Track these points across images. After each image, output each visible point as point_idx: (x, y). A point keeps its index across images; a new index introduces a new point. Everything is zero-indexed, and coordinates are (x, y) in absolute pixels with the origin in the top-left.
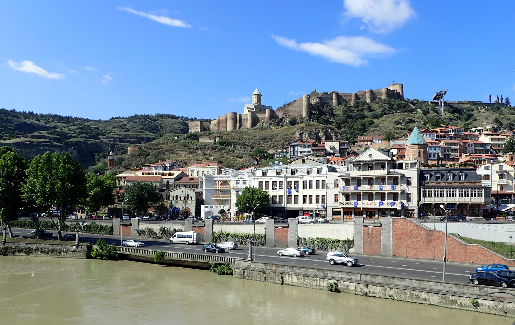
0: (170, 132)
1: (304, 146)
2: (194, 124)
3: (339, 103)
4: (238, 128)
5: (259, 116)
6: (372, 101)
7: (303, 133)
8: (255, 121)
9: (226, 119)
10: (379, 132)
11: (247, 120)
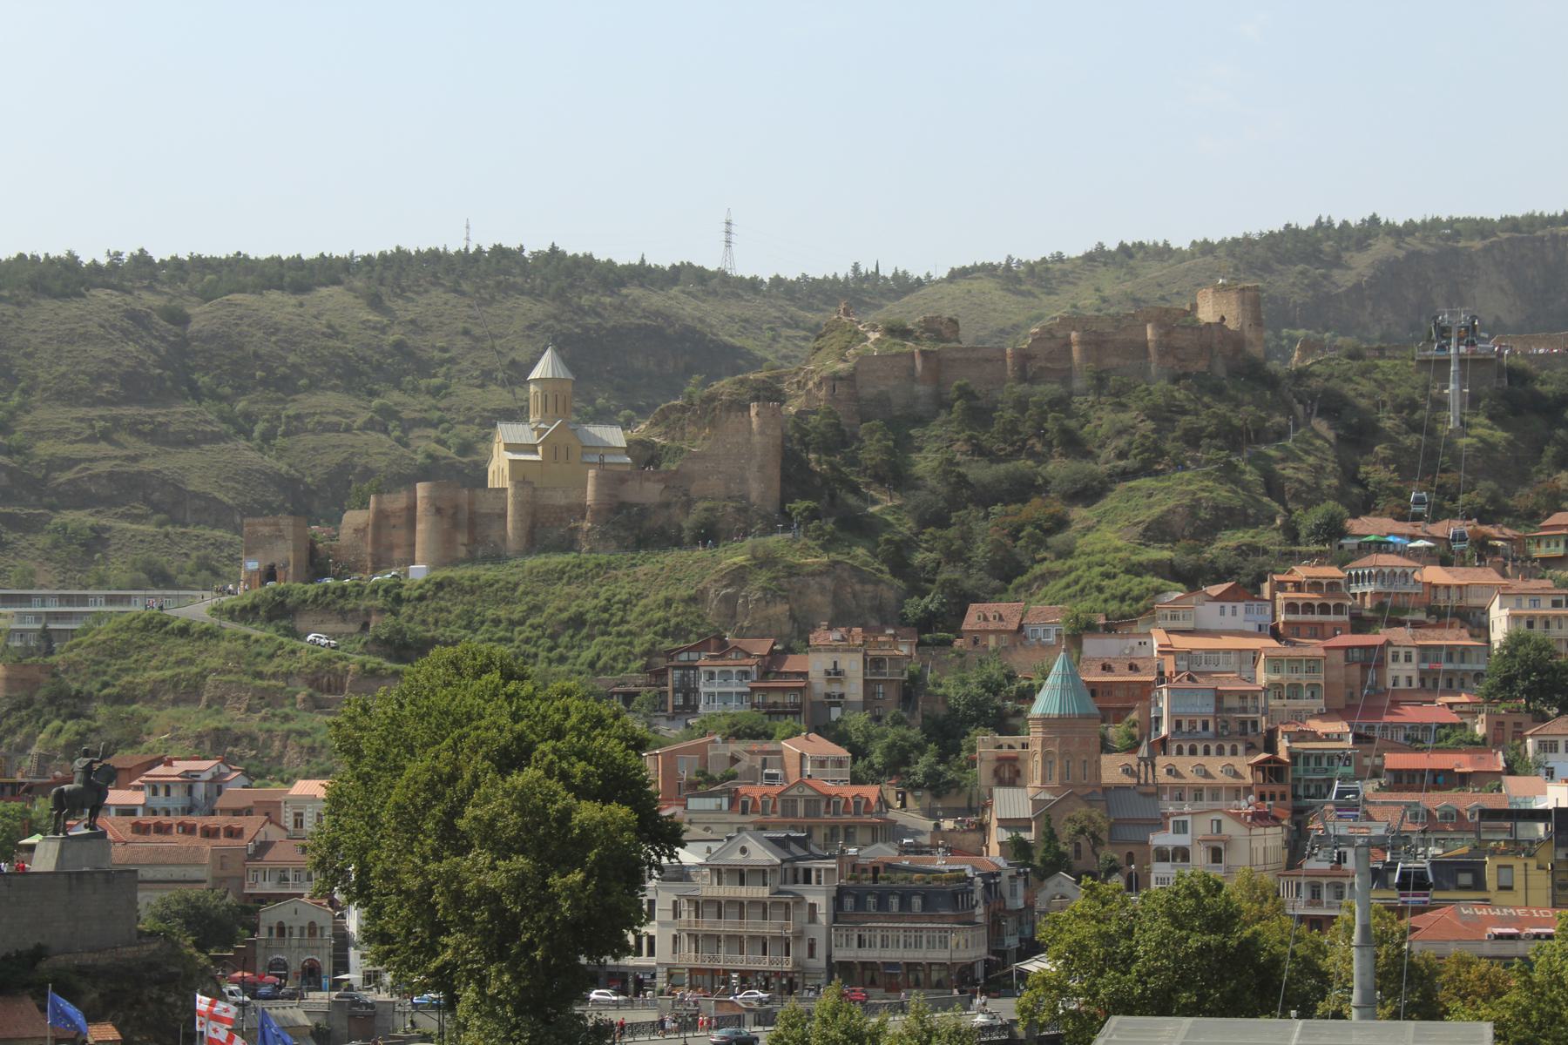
2: (266, 530)
4: (462, 552)
7: (734, 597)
9: (412, 508)
11: (503, 516)
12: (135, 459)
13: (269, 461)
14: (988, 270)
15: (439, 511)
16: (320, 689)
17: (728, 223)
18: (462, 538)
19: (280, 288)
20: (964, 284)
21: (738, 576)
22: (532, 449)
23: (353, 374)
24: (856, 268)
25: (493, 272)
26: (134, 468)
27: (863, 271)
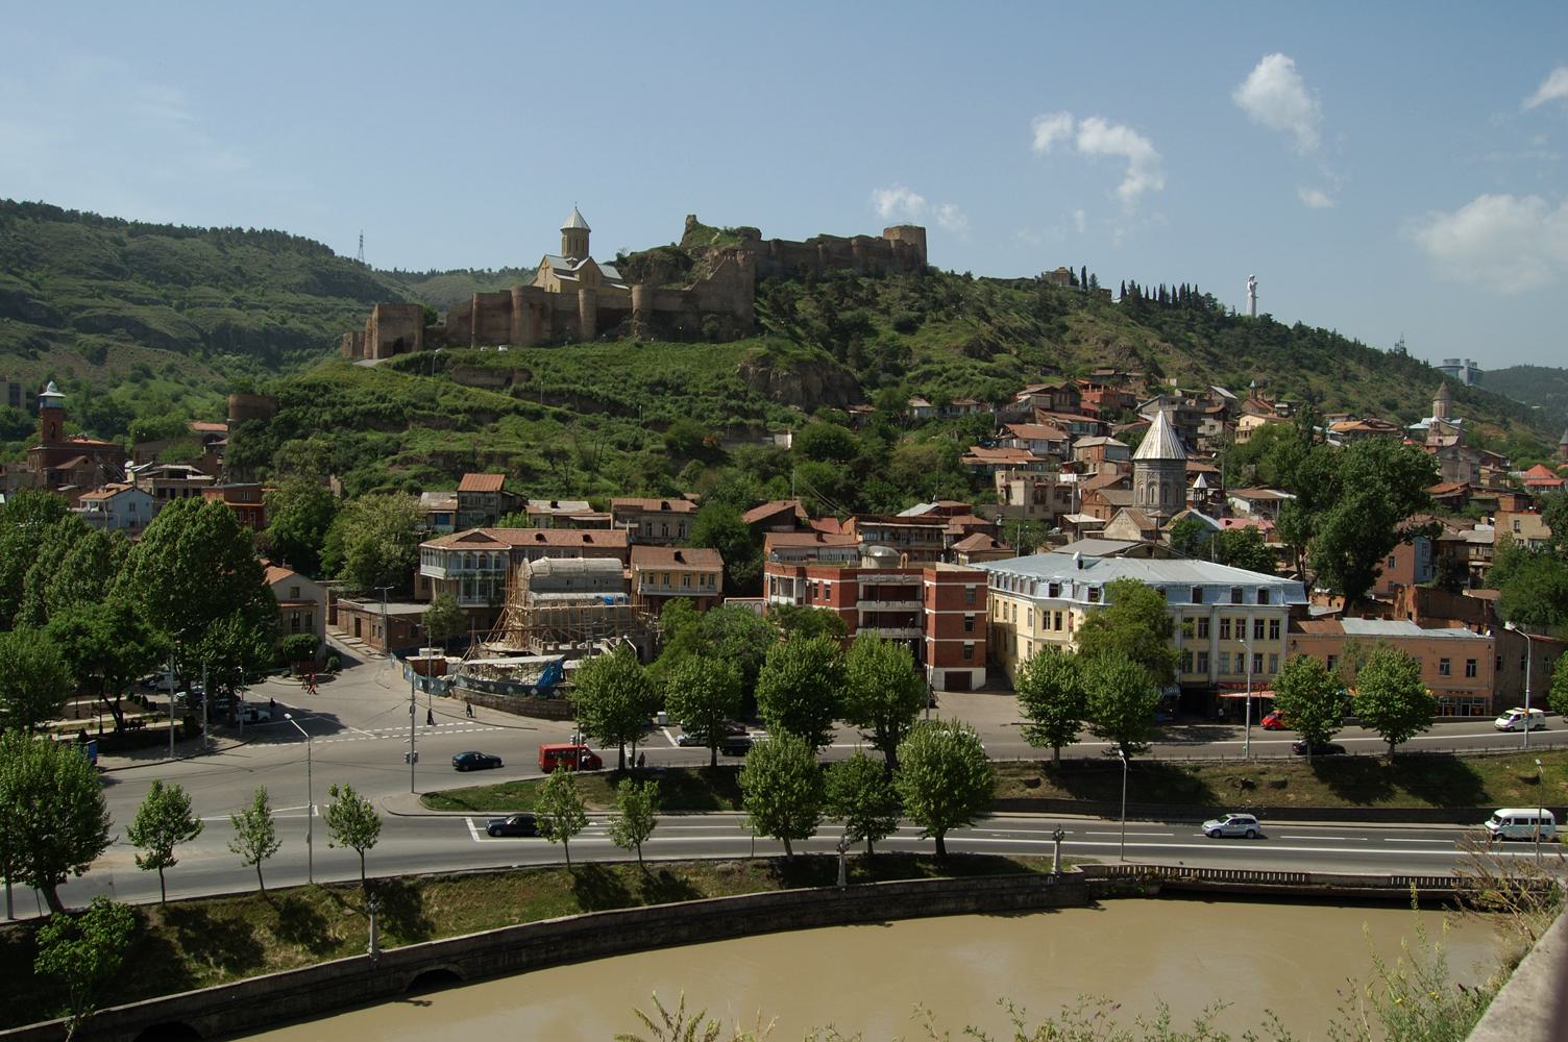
0: (69, 272)
11: (576, 312)
12: (119, 309)
13: (182, 316)
15: (532, 306)
18: (547, 326)
19: (168, 235)
21: (765, 360)
22: (571, 274)
23: (215, 279)
25: (274, 241)
26: (120, 314)
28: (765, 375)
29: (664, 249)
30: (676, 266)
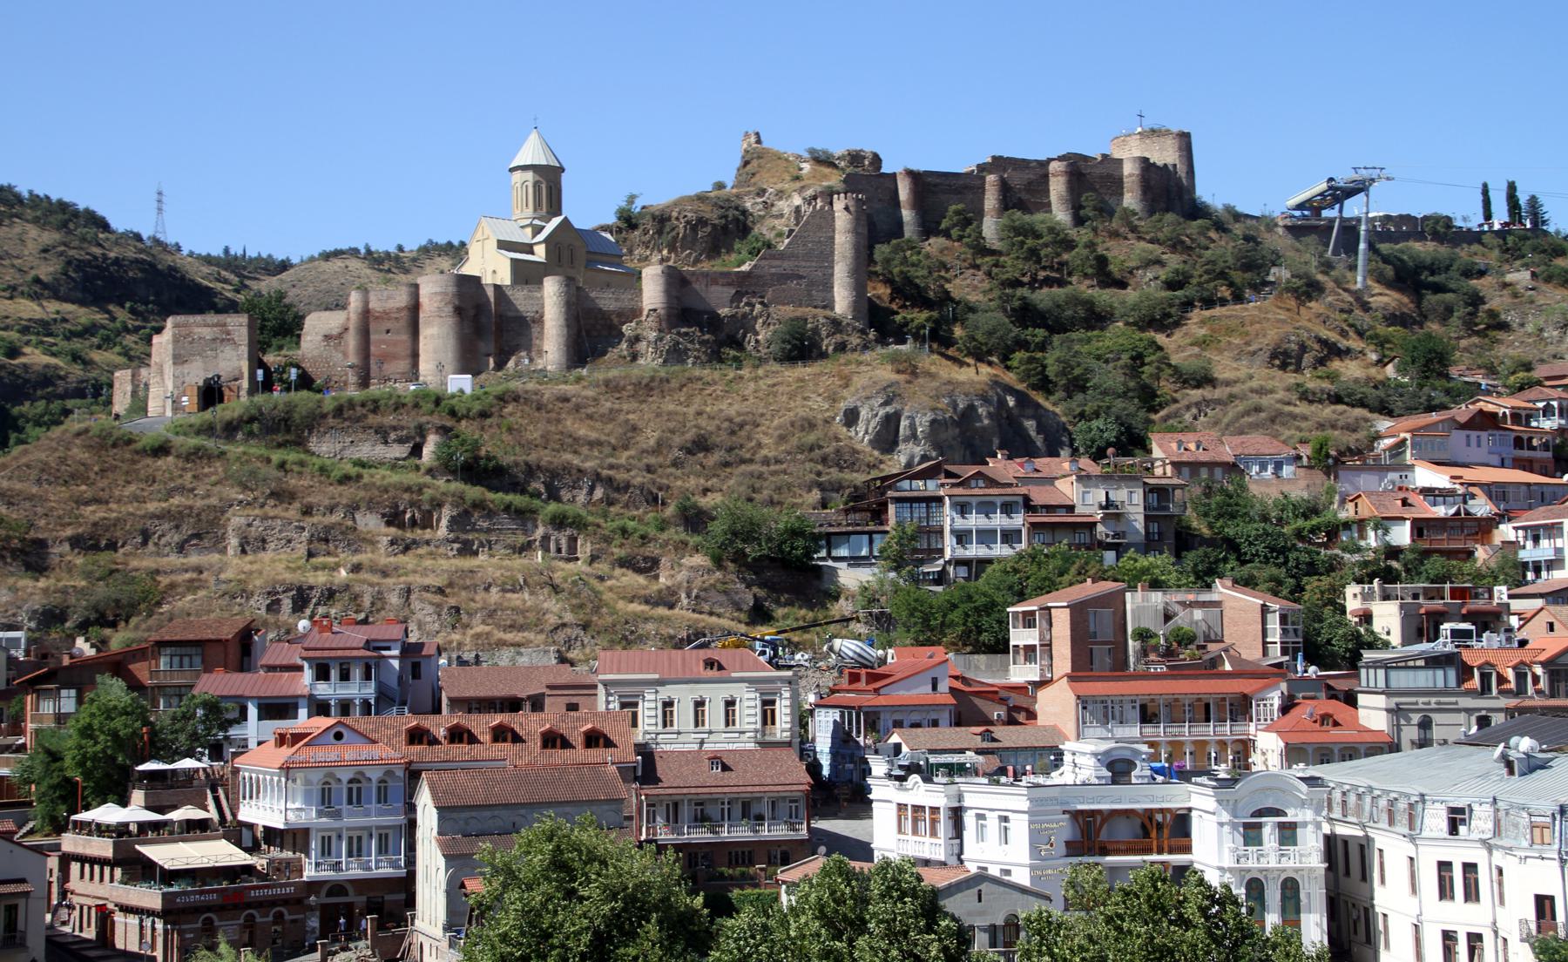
1: (986, 508)
2: (207, 333)
3: (929, 228)
5: (607, 301)
6: (1079, 221)
8: (591, 335)
9: (415, 308)
10: (1232, 412)
11: (539, 320)
14: (354, 252)
15: (459, 311)
16: (401, 526)
17: (160, 193)
20: (337, 264)
22: (529, 249)
24: (227, 250)
27: (232, 252)
28: (891, 422)
29: (701, 198)
30: (725, 228)
